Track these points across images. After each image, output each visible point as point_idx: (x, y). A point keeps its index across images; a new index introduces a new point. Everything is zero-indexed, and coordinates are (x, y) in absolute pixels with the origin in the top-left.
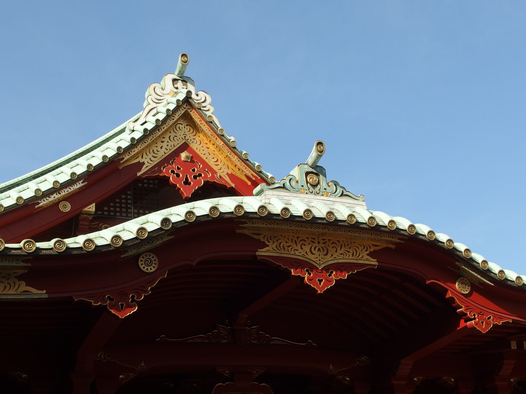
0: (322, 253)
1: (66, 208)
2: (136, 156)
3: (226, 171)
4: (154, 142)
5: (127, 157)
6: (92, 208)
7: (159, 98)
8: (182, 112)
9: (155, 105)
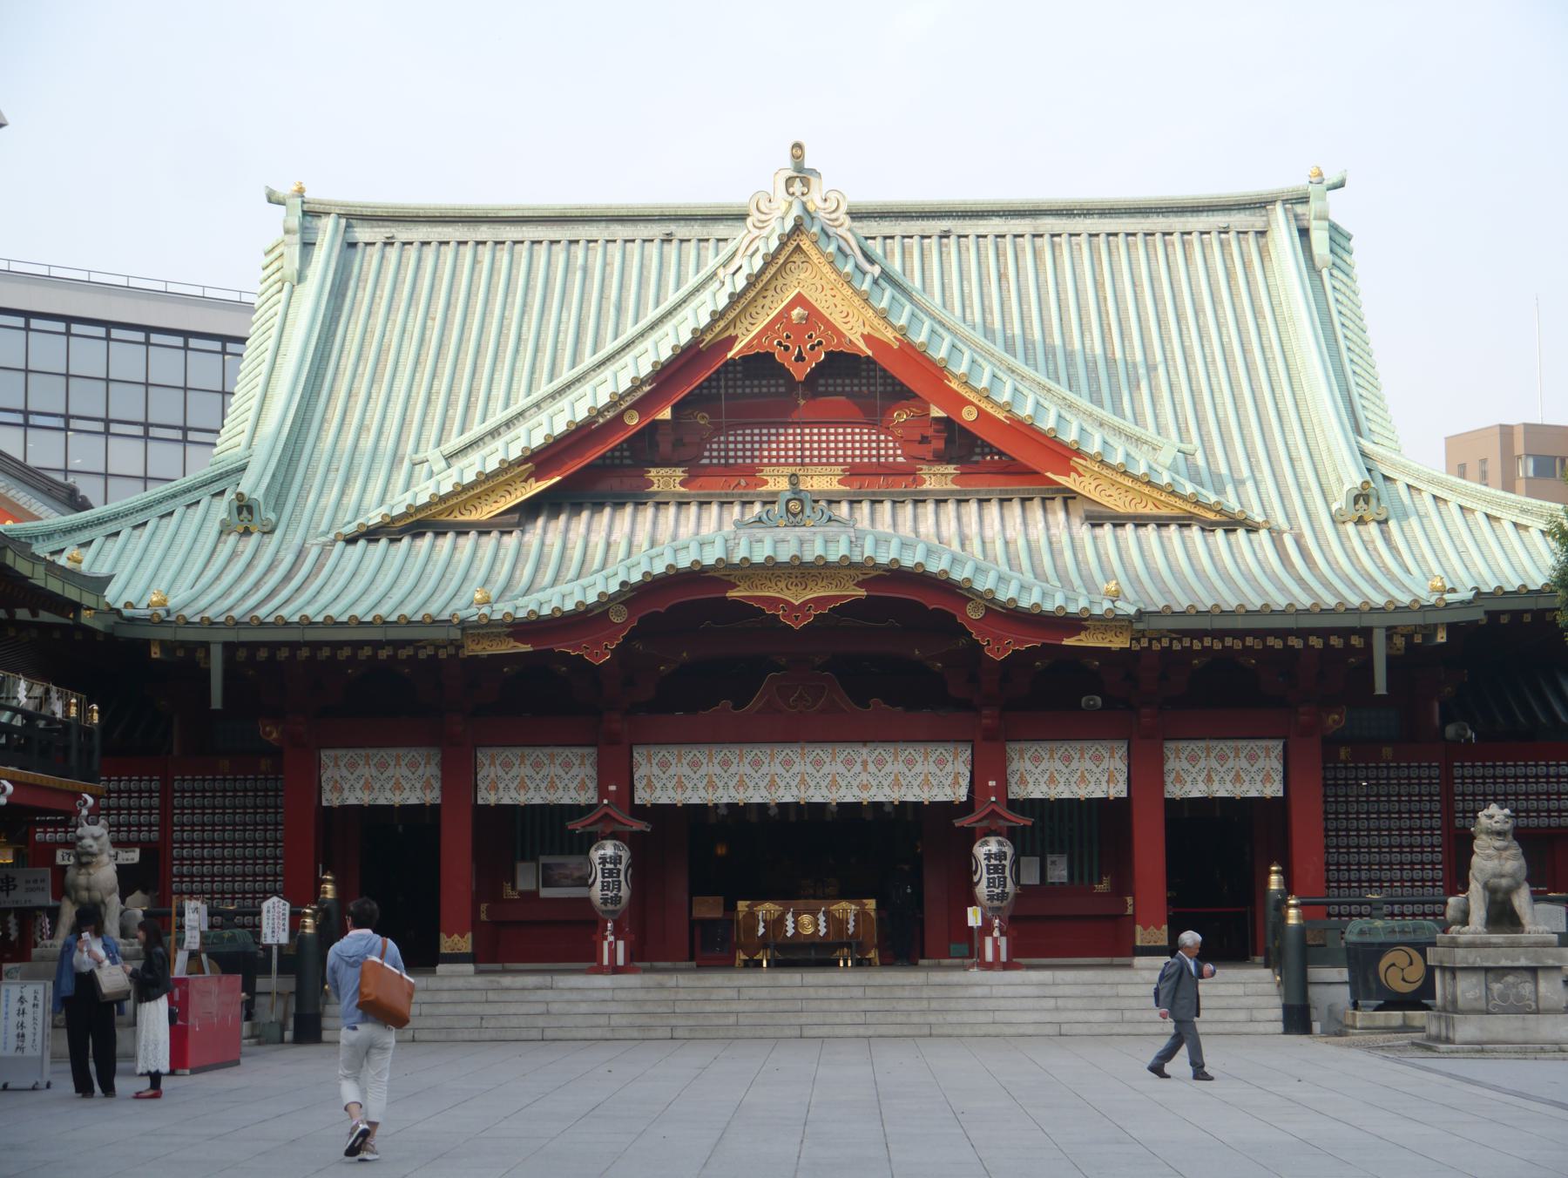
1: (633, 420)
2: (726, 328)
4: (754, 299)
5: (708, 337)
6: (666, 414)
7: (763, 217)
8: (790, 248)
9: (756, 232)
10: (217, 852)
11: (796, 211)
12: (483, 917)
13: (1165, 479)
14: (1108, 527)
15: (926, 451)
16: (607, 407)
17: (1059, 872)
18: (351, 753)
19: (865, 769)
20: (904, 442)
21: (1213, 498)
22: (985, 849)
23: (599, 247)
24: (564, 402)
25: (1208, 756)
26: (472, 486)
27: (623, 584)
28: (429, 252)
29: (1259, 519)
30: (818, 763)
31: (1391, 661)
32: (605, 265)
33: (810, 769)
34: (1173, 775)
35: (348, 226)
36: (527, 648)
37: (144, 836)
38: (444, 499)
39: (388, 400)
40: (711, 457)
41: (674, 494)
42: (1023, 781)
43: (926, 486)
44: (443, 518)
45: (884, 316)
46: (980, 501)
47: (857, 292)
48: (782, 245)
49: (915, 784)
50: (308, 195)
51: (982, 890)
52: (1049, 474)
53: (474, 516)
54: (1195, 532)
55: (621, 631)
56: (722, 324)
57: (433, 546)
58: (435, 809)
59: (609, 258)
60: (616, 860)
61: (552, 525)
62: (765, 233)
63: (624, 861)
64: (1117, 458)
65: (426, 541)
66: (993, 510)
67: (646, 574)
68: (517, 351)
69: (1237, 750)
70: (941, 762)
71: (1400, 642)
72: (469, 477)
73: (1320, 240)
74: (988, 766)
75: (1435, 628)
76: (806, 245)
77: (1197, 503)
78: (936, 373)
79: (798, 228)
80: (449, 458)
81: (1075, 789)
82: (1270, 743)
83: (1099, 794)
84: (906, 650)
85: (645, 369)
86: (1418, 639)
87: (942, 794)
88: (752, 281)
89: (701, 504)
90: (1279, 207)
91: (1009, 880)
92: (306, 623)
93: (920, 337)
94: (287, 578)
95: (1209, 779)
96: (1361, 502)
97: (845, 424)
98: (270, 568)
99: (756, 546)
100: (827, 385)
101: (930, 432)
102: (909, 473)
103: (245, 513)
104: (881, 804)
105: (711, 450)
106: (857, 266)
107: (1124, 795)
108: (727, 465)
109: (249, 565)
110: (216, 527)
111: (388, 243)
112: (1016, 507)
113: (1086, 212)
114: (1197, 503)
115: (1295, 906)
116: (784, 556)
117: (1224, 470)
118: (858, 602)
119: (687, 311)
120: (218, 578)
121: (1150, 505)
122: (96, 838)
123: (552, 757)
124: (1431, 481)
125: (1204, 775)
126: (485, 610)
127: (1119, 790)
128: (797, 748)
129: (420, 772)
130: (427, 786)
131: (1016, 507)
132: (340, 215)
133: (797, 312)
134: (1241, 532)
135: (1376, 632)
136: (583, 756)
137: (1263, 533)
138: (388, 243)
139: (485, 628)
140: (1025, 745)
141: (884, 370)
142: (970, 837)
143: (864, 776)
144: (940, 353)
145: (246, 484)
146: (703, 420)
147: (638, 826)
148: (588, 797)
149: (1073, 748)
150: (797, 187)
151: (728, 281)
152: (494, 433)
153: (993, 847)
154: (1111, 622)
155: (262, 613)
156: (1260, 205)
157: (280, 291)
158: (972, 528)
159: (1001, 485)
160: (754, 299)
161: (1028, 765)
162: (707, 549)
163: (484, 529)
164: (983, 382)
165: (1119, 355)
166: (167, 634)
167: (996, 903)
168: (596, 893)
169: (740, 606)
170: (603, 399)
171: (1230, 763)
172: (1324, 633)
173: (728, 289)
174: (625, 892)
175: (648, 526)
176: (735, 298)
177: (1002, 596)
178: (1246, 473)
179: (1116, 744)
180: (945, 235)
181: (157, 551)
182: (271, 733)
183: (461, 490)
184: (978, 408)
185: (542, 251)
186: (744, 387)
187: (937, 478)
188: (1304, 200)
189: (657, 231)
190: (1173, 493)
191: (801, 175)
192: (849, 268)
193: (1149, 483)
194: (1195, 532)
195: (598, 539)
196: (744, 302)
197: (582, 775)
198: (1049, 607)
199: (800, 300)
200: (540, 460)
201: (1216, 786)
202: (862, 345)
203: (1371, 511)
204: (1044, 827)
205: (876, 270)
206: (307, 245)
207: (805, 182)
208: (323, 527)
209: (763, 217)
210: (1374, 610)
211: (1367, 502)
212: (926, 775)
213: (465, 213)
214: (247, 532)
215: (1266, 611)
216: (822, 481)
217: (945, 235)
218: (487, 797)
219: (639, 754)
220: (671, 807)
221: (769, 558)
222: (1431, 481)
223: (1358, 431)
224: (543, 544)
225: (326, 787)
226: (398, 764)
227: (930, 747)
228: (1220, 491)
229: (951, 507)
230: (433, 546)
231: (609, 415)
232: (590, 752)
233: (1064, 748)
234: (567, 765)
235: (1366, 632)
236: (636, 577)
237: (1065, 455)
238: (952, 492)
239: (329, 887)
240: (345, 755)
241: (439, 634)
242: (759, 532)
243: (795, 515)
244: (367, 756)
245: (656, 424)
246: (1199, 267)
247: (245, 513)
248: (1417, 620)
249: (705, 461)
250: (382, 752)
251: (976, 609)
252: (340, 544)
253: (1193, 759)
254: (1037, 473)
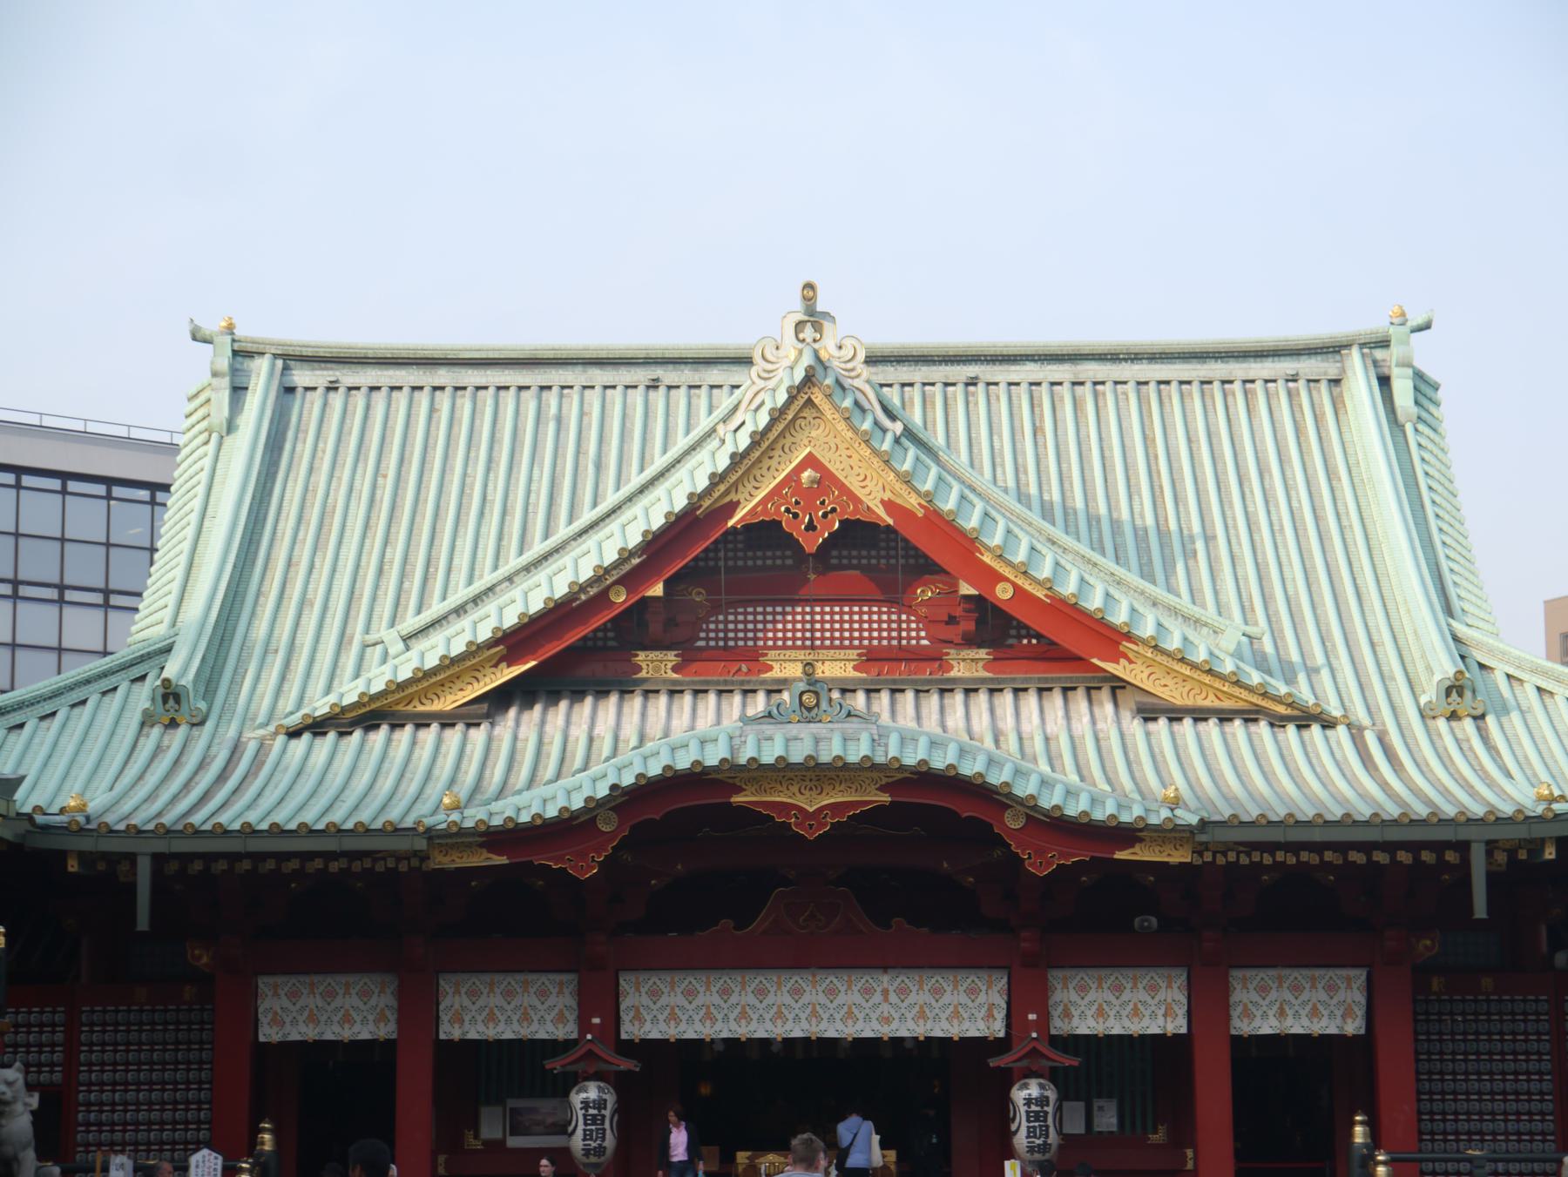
0: (814, 793)
1: (620, 597)
2: (727, 492)
3: (880, 495)
4: (759, 460)
5: (707, 503)
6: (657, 590)
7: (769, 367)
9: (761, 384)
10: (131, 1096)
11: (807, 360)
12: (441, 1170)
13: (1228, 667)
14: (1162, 722)
15: (954, 633)
16: (591, 582)
17: (1107, 1120)
18: (293, 980)
19: (886, 999)
20: (928, 622)
21: (1283, 689)
22: (1025, 1093)
23: (575, 395)
24: (541, 576)
25: (1280, 986)
26: (434, 671)
27: (614, 787)
28: (379, 399)
29: (1336, 712)
30: (832, 992)
31: (1492, 879)
32: (582, 414)
33: (822, 999)
34: (1240, 1009)
35: (286, 368)
36: (502, 860)
37: (44, 1078)
38: (402, 686)
39: (334, 570)
40: (708, 639)
41: (665, 681)
42: (1067, 1014)
43: (953, 674)
44: (400, 708)
45: (907, 479)
46: (1016, 691)
47: (876, 452)
48: (791, 399)
49: (943, 1016)
50: (239, 333)
51: (1021, 1140)
52: (1095, 661)
53: (437, 706)
54: (1263, 728)
55: (613, 840)
56: (722, 488)
57: (389, 741)
58: (389, 1044)
59: (589, 407)
60: (600, 1104)
61: (526, 716)
62: (771, 384)
63: (609, 1106)
64: (1173, 643)
65: (379, 737)
66: (1031, 701)
67: (640, 776)
68: (481, 514)
69: (1313, 979)
70: (972, 992)
71: (1501, 857)
72: (431, 662)
73: (1403, 389)
74: (1027, 997)
75: (1542, 842)
76: (818, 398)
77: (1265, 695)
78: (967, 544)
79: (809, 379)
80: (407, 639)
81: (1127, 1023)
82: (1353, 972)
83: (1154, 1030)
84: (938, 863)
85: (634, 539)
86: (1523, 855)
87: (975, 1027)
88: (758, 439)
89: (696, 692)
90: (1355, 352)
91: (1052, 1130)
92: (249, 831)
93: (948, 504)
94: (222, 777)
95: (1282, 1013)
96: (1454, 695)
97: (861, 602)
98: (202, 766)
99: (765, 744)
100: (840, 557)
101: (958, 612)
102: (933, 658)
103: (171, 702)
104: (902, 1039)
105: (708, 631)
106: (876, 423)
107: (1184, 1030)
108: (726, 648)
109: (177, 762)
110: (136, 718)
111: (332, 388)
112: (1057, 698)
113: (1134, 357)
114: (1265, 695)
115: (1384, 1163)
116: (797, 757)
117: (1295, 657)
118: (880, 808)
119: (681, 473)
120: (141, 777)
121: (1211, 697)
122: (9, 1084)
123: (526, 984)
124: (1535, 670)
125: (1275, 1008)
126: (455, 817)
127: (1177, 1025)
128: (807, 974)
129: (373, 1002)
130: (381, 1018)
131: (1057, 698)
132: (275, 356)
133: (807, 475)
134: (1316, 729)
135: (1474, 846)
136: (561, 984)
137: (1341, 730)
138: (332, 388)
139: (456, 838)
140: (1068, 973)
141: (905, 540)
142: (1007, 1079)
143: (885, 1008)
144: (971, 522)
145: (172, 669)
146: (698, 596)
147: (626, 1065)
148: (566, 1031)
149: (1123, 976)
150: (808, 333)
151: (729, 438)
152: (460, 611)
153: (1034, 1090)
154: (1171, 833)
155: (197, 819)
156: (1333, 349)
157: (206, 443)
158: (1008, 723)
159: (1040, 673)
160: (759, 460)
161: (1074, 996)
162: (709, 747)
163: (447, 721)
164: (1021, 556)
165: (1173, 525)
166: (86, 845)
167: (1037, 1156)
168: (577, 1142)
169: (745, 811)
170: (586, 574)
171: (1305, 996)
172: (1414, 847)
173: (729, 448)
174: (610, 1142)
175: (636, 717)
176: (737, 459)
177: (1046, 803)
178: (1320, 659)
179: (1174, 972)
180: (972, 382)
181: (68, 746)
182: (199, 958)
183: (422, 676)
184: (1015, 585)
185: (509, 398)
186: (745, 558)
187: (966, 664)
188: (1384, 343)
189: (641, 375)
190: (1237, 683)
191: (813, 318)
192: (867, 425)
193: (1210, 672)
194: (1263, 728)
195: (579, 732)
196: (747, 462)
197: (560, 1006)
198: (1099, 815)
199: (810, 461)
200: (512, 642)
201: (1289, 1021)
202: (881, 512)
203: (1466, 704)
204: (1093, 1066)
205: (898, 427)
206: (238, 390)
207: (818, 327)
208: (261, 719)
209: (769, 367)
210: (1471, 822)
211: (1461, 695)
212: (956, 1007)
213: (420, 354)
214: (173, 724)
215: (1348, 822)
216: (836, 668)
217: (972, 382)
218: (450, 1031)
219: (626, 982)
220: (662, 1043)
221: (780, 759)
222: (1535, 670)
223: (1449, 611)
224: (515, 738)
225: (264, 1019)
226: (347, 993)
227: (961, 974)
228: (1290, 680)
229: (983, 697)
230: (389, 741)
231: (592, 591)
232: (570, 979)
233: (1113, 976)
234: (543, 994)
235: (1463, 847)
236: (628, 780)
237: (1113, 639)
238: (983, 681)
239: (267, 1137)
240: (287, 983)
241: (402, 845)
242: (768, 729)
243: (809, 709)
244: (312, 985)
245: (645, 601)
246: (1263, 421)
247: (171, 702)
248: (1521, 833)
249: (701, 643)
250: (329, 979)
251: (1015, 817)
252: (281, 739)
253: (1263, 990)
254: (1080, 659)
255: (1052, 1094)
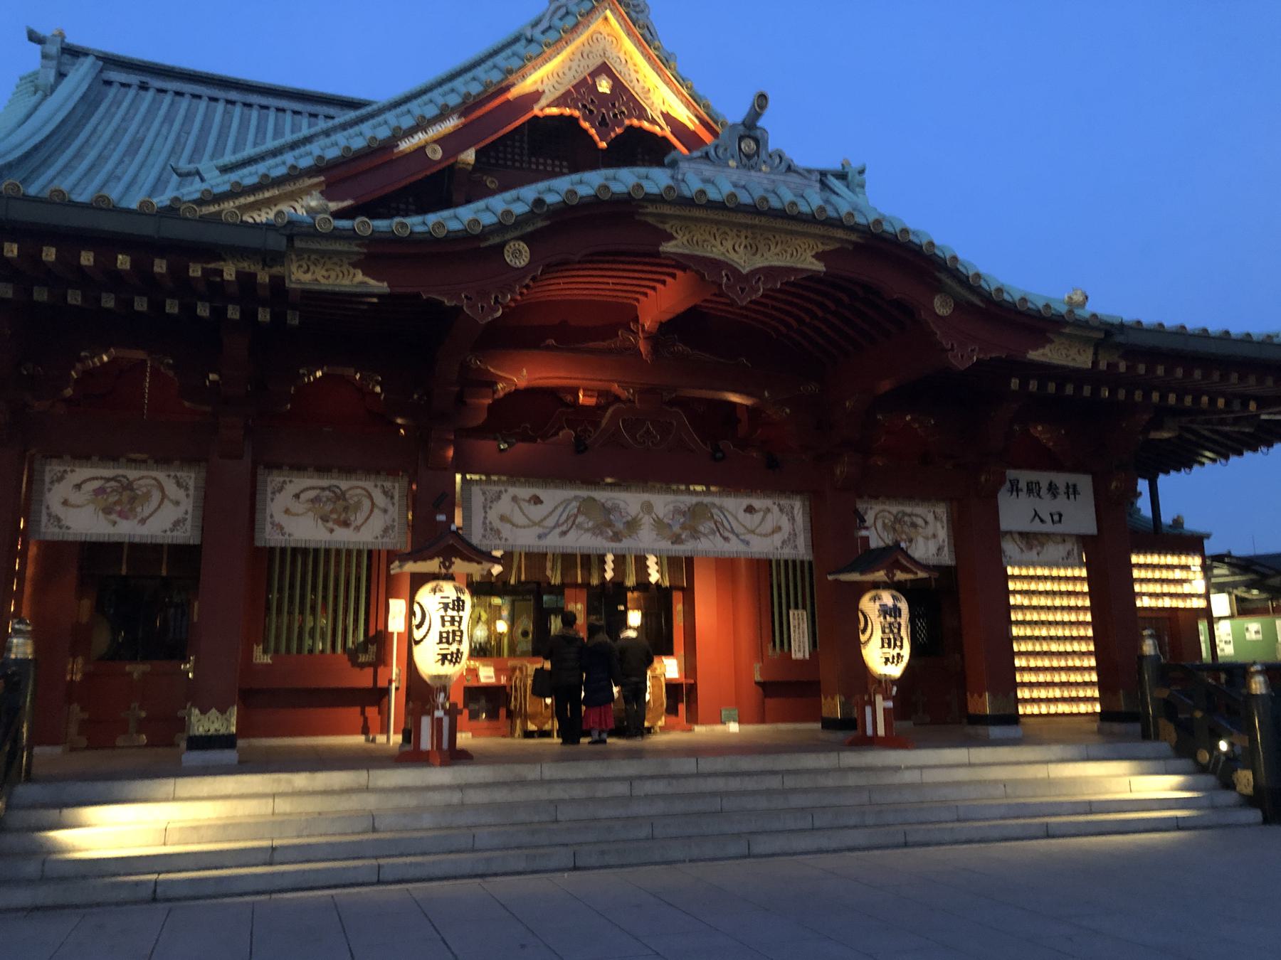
6: (469, 156)
50: (67, 40)
80: (225, 170)
111: (144, 87)
132: (98, 58)
243: (748, 157)
255: (904, 606)
